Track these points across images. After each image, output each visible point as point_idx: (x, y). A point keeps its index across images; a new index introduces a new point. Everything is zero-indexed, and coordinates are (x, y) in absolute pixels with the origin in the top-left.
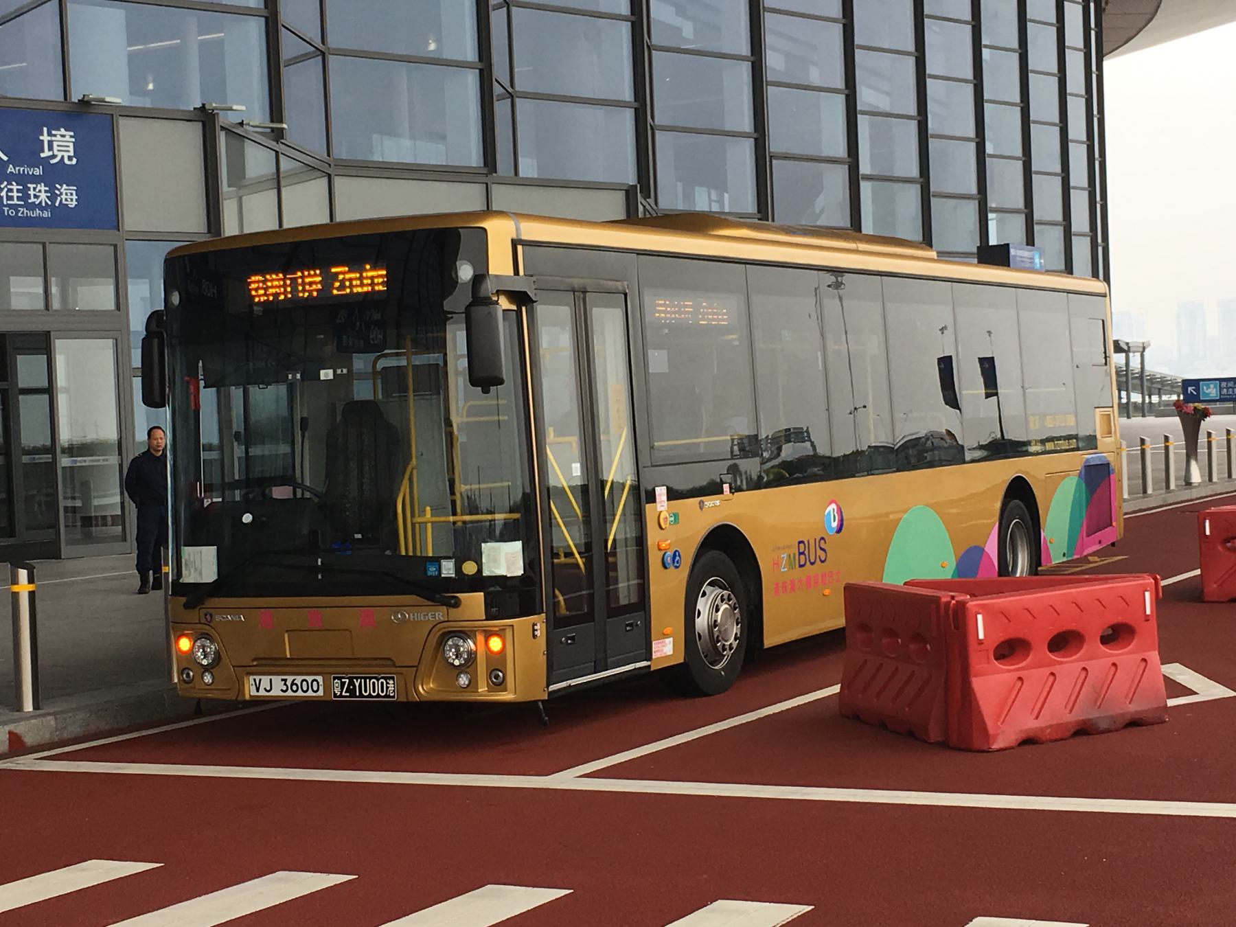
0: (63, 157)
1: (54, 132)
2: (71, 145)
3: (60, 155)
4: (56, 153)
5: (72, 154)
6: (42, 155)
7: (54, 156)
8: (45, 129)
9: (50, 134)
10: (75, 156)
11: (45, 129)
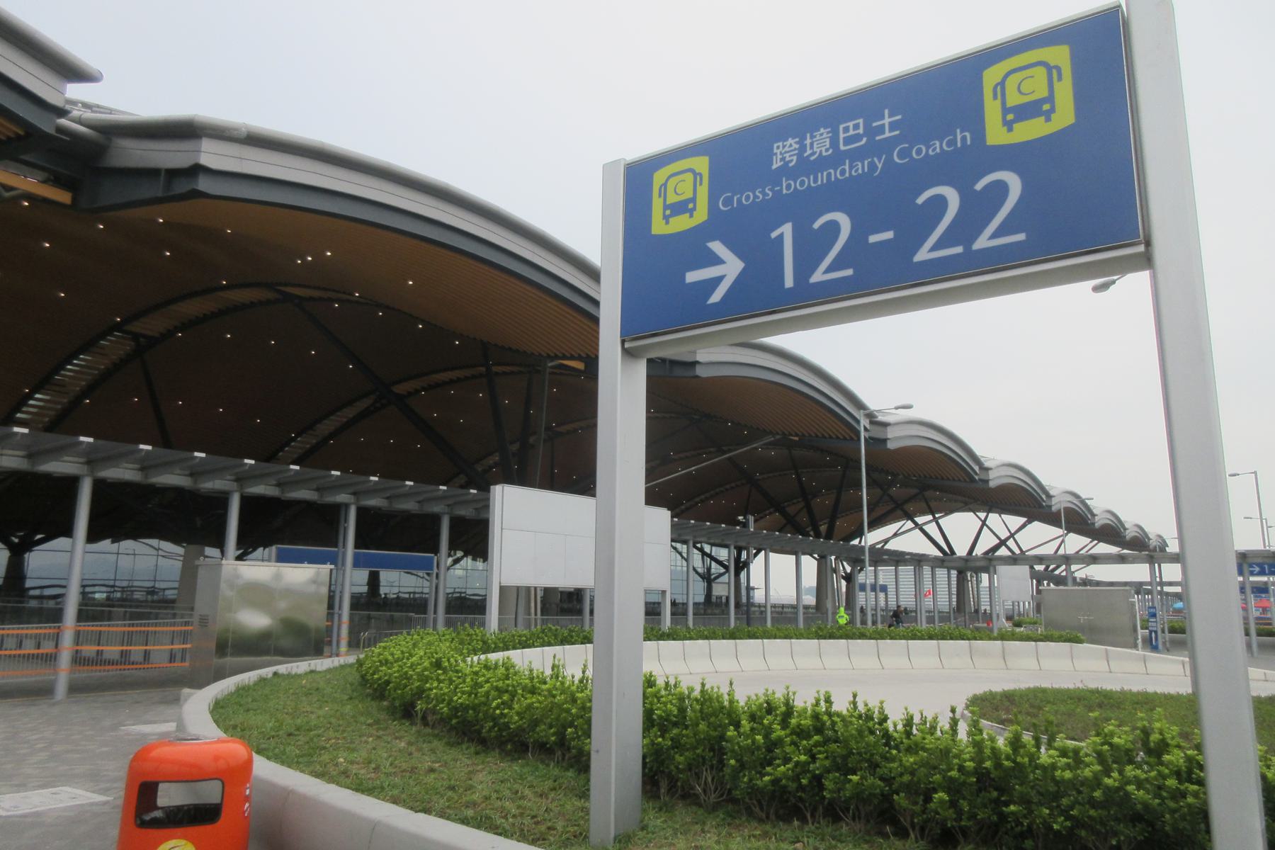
0: (821, 151)
1: (815, 134)
2: (828, 140)
3: (818, 150)
4: (815, 150)
5: (828, 146)
6: (805, 155)
7: (813, 153)
8: (808, 135)
9: (812, 137)
10: (831, 147)
11: (808, 135)
